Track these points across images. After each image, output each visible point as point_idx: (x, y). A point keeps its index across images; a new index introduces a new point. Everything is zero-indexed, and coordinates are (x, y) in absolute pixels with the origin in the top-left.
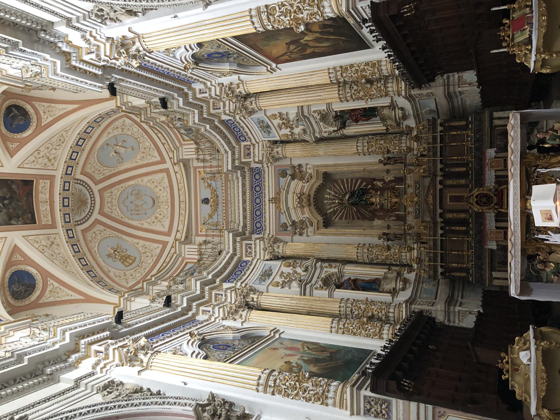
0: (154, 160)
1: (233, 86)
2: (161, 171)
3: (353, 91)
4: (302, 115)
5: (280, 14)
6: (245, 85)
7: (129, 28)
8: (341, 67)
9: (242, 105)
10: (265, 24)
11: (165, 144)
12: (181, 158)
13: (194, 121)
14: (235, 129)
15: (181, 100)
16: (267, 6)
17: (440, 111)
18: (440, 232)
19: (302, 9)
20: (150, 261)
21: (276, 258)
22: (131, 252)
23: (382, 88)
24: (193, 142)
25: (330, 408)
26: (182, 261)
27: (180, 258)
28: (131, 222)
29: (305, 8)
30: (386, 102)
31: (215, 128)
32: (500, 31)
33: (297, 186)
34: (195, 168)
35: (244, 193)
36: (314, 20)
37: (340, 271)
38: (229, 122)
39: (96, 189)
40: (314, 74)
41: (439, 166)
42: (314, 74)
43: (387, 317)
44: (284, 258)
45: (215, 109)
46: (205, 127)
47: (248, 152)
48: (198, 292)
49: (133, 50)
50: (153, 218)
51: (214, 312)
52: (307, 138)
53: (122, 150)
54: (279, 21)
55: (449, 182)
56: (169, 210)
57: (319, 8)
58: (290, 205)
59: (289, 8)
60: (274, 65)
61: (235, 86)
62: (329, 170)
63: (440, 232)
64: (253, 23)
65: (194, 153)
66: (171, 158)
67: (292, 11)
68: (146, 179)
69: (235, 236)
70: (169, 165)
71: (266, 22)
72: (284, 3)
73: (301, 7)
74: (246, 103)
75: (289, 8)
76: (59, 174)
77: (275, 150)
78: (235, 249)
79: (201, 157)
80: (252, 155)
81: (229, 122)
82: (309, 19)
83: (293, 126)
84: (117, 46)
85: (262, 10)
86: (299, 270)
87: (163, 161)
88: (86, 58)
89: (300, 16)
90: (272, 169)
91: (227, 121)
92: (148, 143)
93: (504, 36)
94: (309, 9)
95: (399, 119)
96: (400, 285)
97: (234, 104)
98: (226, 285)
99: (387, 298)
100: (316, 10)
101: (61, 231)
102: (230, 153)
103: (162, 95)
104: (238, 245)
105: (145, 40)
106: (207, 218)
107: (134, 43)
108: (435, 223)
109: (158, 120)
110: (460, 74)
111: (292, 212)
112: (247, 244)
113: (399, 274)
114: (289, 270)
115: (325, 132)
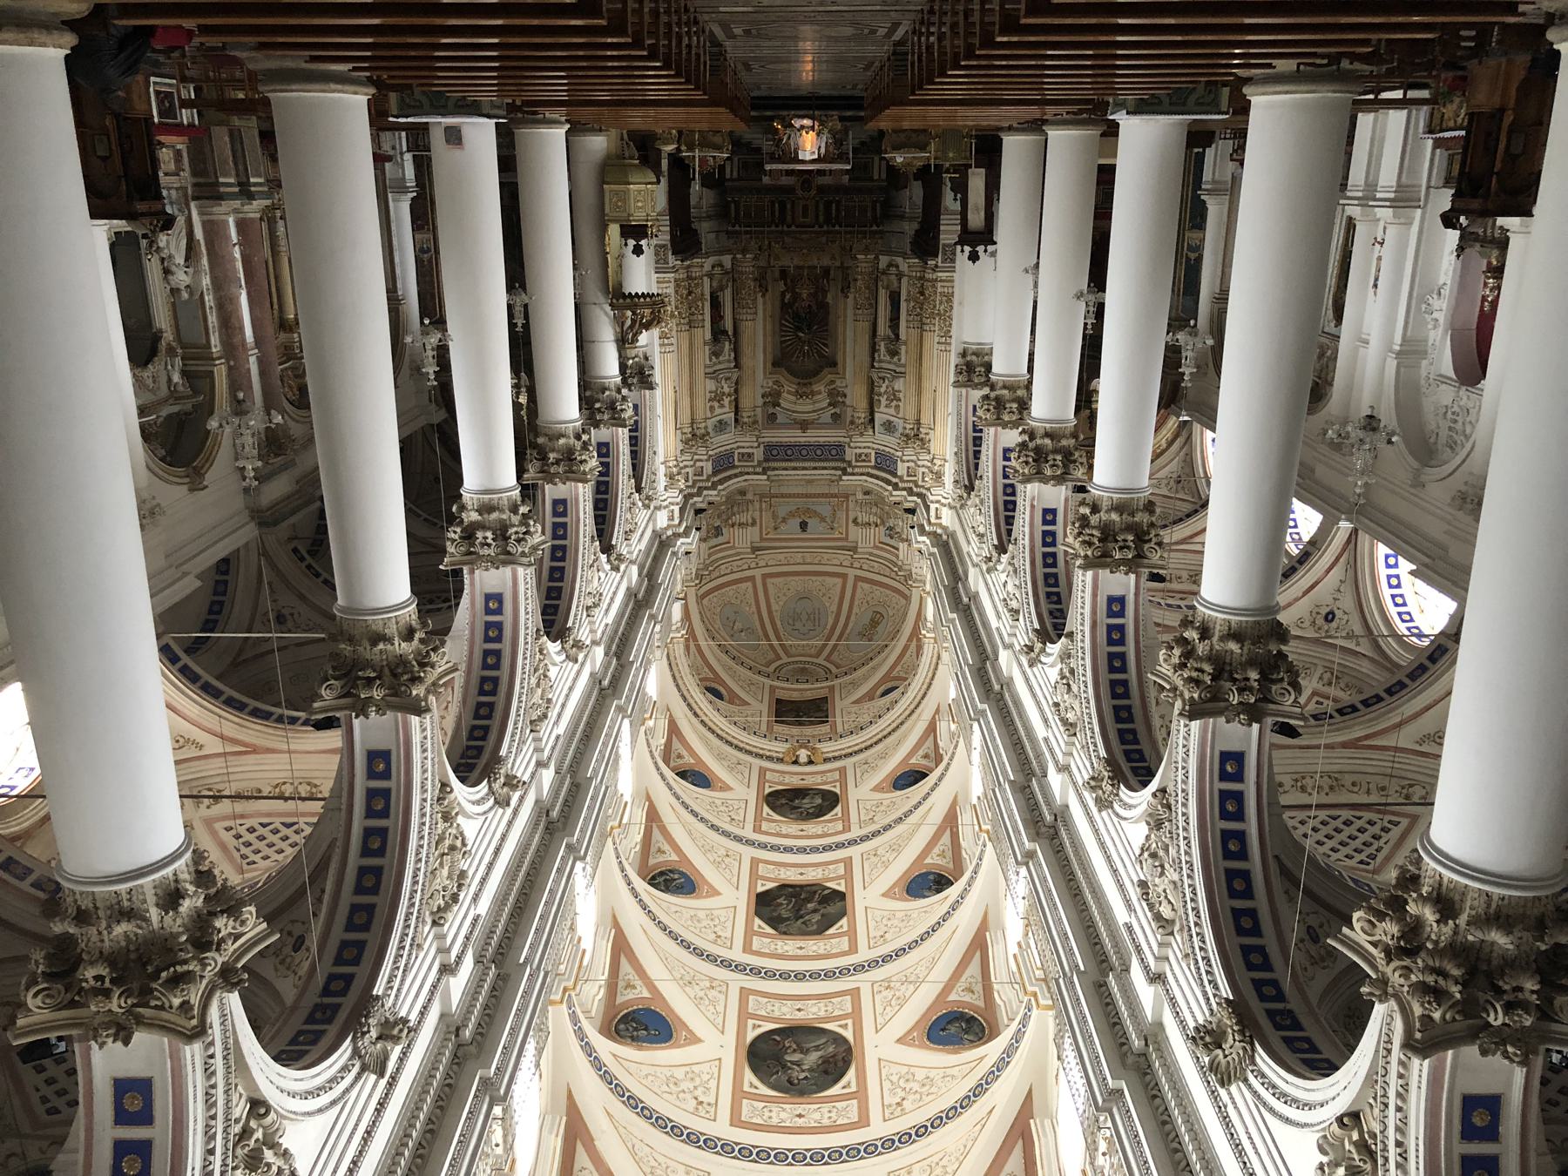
0: (751, 590)
2: (765, 585)
4: (712, 375)
18: (837, 228)
20: (878, 593)
21: (872, 421)
22: (866, 620)
25: (956, 290)
27: (875, 552)
28: (829, 627)
31: (721, 482)
33: (787, 400)
34: (762, 539)
35: (795, 469)
37: (883, 340)
39: (785, 659)
41: (773, 228)
44: (872, 413)
48: (905, 493)
51: (938, 502)
52: (735, 377)
53: (738, 626)
55: (789, 218)
56: (814, 578)
58: (810, 408)
62: (770, 358)
63: (837, 228)
66: (749, 568)
68: (775, 607)
69: (845, 472)
70: (758, 573)
76: (768, 682)
77: (746, 420)
78: (862, 474)
79: (750, 521)
80: (750, 450)
86: (883, 390)
87: (752, 579)
88: (676, 521)
90: (765, 433)
96: (893, 269)
98: (902, 469)
99: (904, 280)
102: (746, 477)
104: (856, 470)
106: (824, 524)
108: (828, 232)
111: (818, 406)
112: (857, 461)
113: (884, 273)
114: (883, 401)
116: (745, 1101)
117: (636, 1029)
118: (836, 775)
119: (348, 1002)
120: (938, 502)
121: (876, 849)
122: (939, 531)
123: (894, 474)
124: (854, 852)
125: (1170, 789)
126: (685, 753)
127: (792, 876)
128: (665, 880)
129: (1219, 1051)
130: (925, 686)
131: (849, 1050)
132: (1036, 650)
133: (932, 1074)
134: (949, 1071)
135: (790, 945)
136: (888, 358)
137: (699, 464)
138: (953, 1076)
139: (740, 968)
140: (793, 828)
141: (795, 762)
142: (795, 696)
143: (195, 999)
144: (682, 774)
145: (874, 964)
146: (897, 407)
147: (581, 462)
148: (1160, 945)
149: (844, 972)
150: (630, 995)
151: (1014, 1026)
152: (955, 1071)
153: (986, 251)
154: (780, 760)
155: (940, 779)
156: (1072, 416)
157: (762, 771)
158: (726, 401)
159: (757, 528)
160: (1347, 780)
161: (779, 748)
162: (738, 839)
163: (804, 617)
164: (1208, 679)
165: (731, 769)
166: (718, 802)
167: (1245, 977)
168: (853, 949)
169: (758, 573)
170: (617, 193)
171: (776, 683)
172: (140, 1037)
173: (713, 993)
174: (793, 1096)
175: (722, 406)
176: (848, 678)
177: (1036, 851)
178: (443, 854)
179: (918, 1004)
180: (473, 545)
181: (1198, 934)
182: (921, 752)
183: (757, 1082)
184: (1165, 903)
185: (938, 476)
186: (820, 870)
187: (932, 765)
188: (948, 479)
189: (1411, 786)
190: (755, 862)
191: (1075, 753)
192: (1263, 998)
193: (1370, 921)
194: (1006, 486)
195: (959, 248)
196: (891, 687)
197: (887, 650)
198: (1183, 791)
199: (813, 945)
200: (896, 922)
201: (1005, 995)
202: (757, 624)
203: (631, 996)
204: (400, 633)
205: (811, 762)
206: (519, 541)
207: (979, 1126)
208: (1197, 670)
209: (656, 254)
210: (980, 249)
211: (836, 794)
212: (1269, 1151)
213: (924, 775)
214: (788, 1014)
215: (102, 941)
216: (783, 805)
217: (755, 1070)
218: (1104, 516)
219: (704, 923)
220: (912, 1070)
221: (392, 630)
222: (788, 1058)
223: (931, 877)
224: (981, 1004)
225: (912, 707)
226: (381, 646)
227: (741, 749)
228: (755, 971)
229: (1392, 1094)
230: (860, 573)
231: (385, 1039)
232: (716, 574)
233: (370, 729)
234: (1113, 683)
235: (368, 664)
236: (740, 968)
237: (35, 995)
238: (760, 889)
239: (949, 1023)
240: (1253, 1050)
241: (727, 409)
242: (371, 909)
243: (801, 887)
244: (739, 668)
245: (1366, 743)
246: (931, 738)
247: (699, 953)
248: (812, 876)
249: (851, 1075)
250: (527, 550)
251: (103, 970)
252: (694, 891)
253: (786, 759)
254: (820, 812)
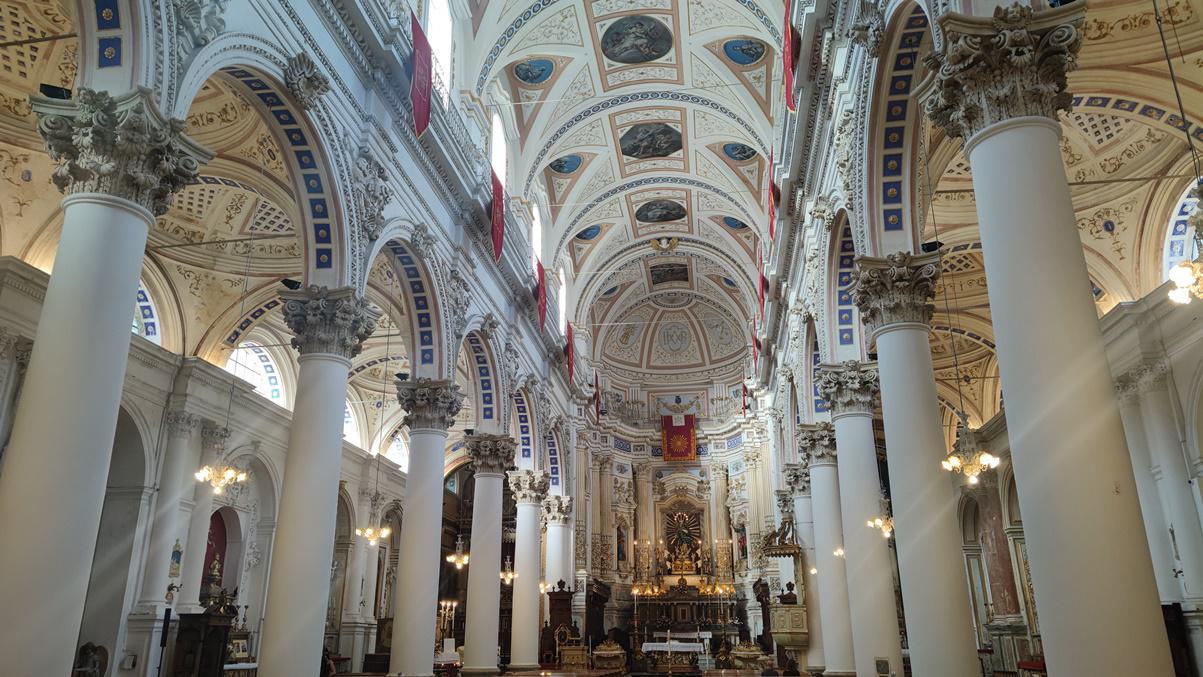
18: (662, 603)
21: (634, 473)
22: (632, 338)
26: (626, 387)
28: (657, 332)
30: (750, 566)
31: (735, 428)
34: (706, 390)
41: (705, 603)
43: (605, 569)
44: (634, 478)
50: (662, 351)
52: (729, 499)
53: (719, 329)
56: (669, 364)
62: (706, 514)
63: (662, 603)
66: (714, 369)
68: (696, 344)
70: (708, 367)
76: (695, 292)
80: (717, 451)
92: (726, 353)
96: (624, 574)
98: (611, 441)
99: (615, 567)
101: (649, 295)
108: (667, 600)
114: (626, 486)
116: (669, 8)
117: (750, 49)
118: (640, 232)
119: (894, 50)
120: (580, 420)
121: (606, 185)
122: (578, 401)
123: (616, 438)
124: (620, 182)
125: (366, 242)
126: (745, 240)
127: (661, 162)
128: (745, 152)
129: (308, 76)
130: (584, 296)
131: (604, 50)
132: (487, 325)
133: (545, 40)
134: (534, 42)
135: (655, 116)
136: (624, 515)
137: (750, 440)
138: (530, 40)
139: (686, 98)
140: (664, 194)
141: (669, 239)
142: (676, 284)
143: (950, 46)
144: (744, 226)
145: (596, 109)
146: (616, 482)
147: (806, 439)
148: (367, 140)
149: (615, 102)
150: (757, 72)
151: (490, 77)
152: (530, 43)
153: (554, 588)
154: (679, 239)
155: (565, 235)
156: (477, 480)
157: (691, 231)
158: (734, 484)
159: (710, 397)
160: (284, 254)
161: (681, 248)
162: (700, 184)
163: (675, 338)
164: (338, 314)
165: (712, 231)
166: (717, 208)
167: (301, 125)
168: (612, 117)
169: (708, 366)
170: (798, 627)
171: (690, 291)
172: (988, 14)
173: (702, 79)
174: (638, 15)
175: (736, 480)
176: (641, 298)
177: (473, 193)
178: (847, 161)
179: (561, 85)
180: (861, 378)
181: (336, 149)
182: (584, 252)
183: (664, 22)
184: (364, 168)
185: (580, 436)
186: (642, 168)
187: (575, 244)
188: (574, 435)
189: (245, 253)
190: (686, 169)
191: (451, 260)
192: (287, 112)
193: (187, 168)
194: (527, 432)
195: (572, 590)
196: (610, 294)
197: (615, 318)
198: (355, 241)
199: (640, 117)
200: (584, 137)
201: (502, 96)
202: (707, 332)
203: (756, 71)
204: (880, 313)
205: (659, 240)
206: (829, 382)
207: (507, 8)
208: (346, 319)
210: (557, 590)
211: (639, 219)
212: (268, 15)
213: (579, 236)
214: (650, 70)
215: (1021, 80)
216: (674, 209)
217: (666, 30)
218: (436, 415)
219: (713, 127)
220: (559, 41)
221: (886, 316)
222: (645, 41)
223: (566, 169)
224: (520, 90)
225: (593, 282)
226: (892, 304)
227: (708, 245)
228: (675, 97)
229: (167, 62)
230: (638, 370)
231: (863, 27)
233: (899, 243)
234: (425, 306)
235: (902, 291)
236: (686, 98)
237: (1069, 37)
238: (680, 152)
239: (540, 75)
240: (285, 79)
242: (890, 117)
243: (653, 156)
244: (716, 301)
245: (273, 278)
246: (578, 262)
247: (715, 106)
248: (648, 164)
249: (601, 34)
250: (824, 376)
251: (1015, 58)
252: (724, 147)
253: (675, 241)
254: (648, 206)
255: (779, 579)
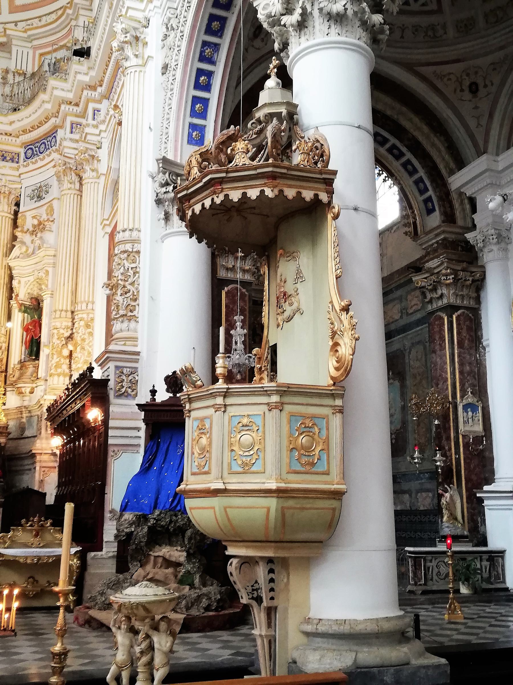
1: (96, 162)
3: (62, 331)
5: (126, 268)
6: (94, 180)
7: (153, 57)
8: (92, 319)
9: (71, 169)
10: (120, 246)
11: (40, 21)
12: (14, 42)
13: (57, 88)
14: (43, 146)
15: (86, 79)
16: (138, 252)
17: (22, 441)
19: (126, 296)
23: (59, 370)
24: (36, 69)
29: (125, 300)
32: (40, 517)
36: (113, 308)
38: (54, 140)
40: (89, 282)
42: (89, 282)
45: (72, 124)
46: (48, 102)
47: (8, 158)
49: (129, 51)
54: (119, 264)
57: (122, 316)
59: (130, 280)
60: (109, 230)
61: (95, 166)
64: (124, 231)
65: (19, 67)
66: (16, 23)
67: (127, 283)
71: (122, 247)
72: (137, 275)
73: (128, 295)
74: (73, 174)
75: (130, 280)
79: (10, 77)
81: (54, 140)
82: (115, 302)
83: (34, 236)
84: (137, 29)
85: (136, 245)
89: (119, 292)
91: (55, 137)
93: (33, 521)
94: (123, 304)
95: (18, 388)
97: (73, 156)
100: (121, 312)
103: (93, 52)
105: (137, 73)
107: (136, 56)
109: (73, 23)
110: (57, 469)
115: (19, 282)
137: (76, 136)
209: (134, 384)
232: (60, 12)
241: (29, 215)
255: (134, 371)
